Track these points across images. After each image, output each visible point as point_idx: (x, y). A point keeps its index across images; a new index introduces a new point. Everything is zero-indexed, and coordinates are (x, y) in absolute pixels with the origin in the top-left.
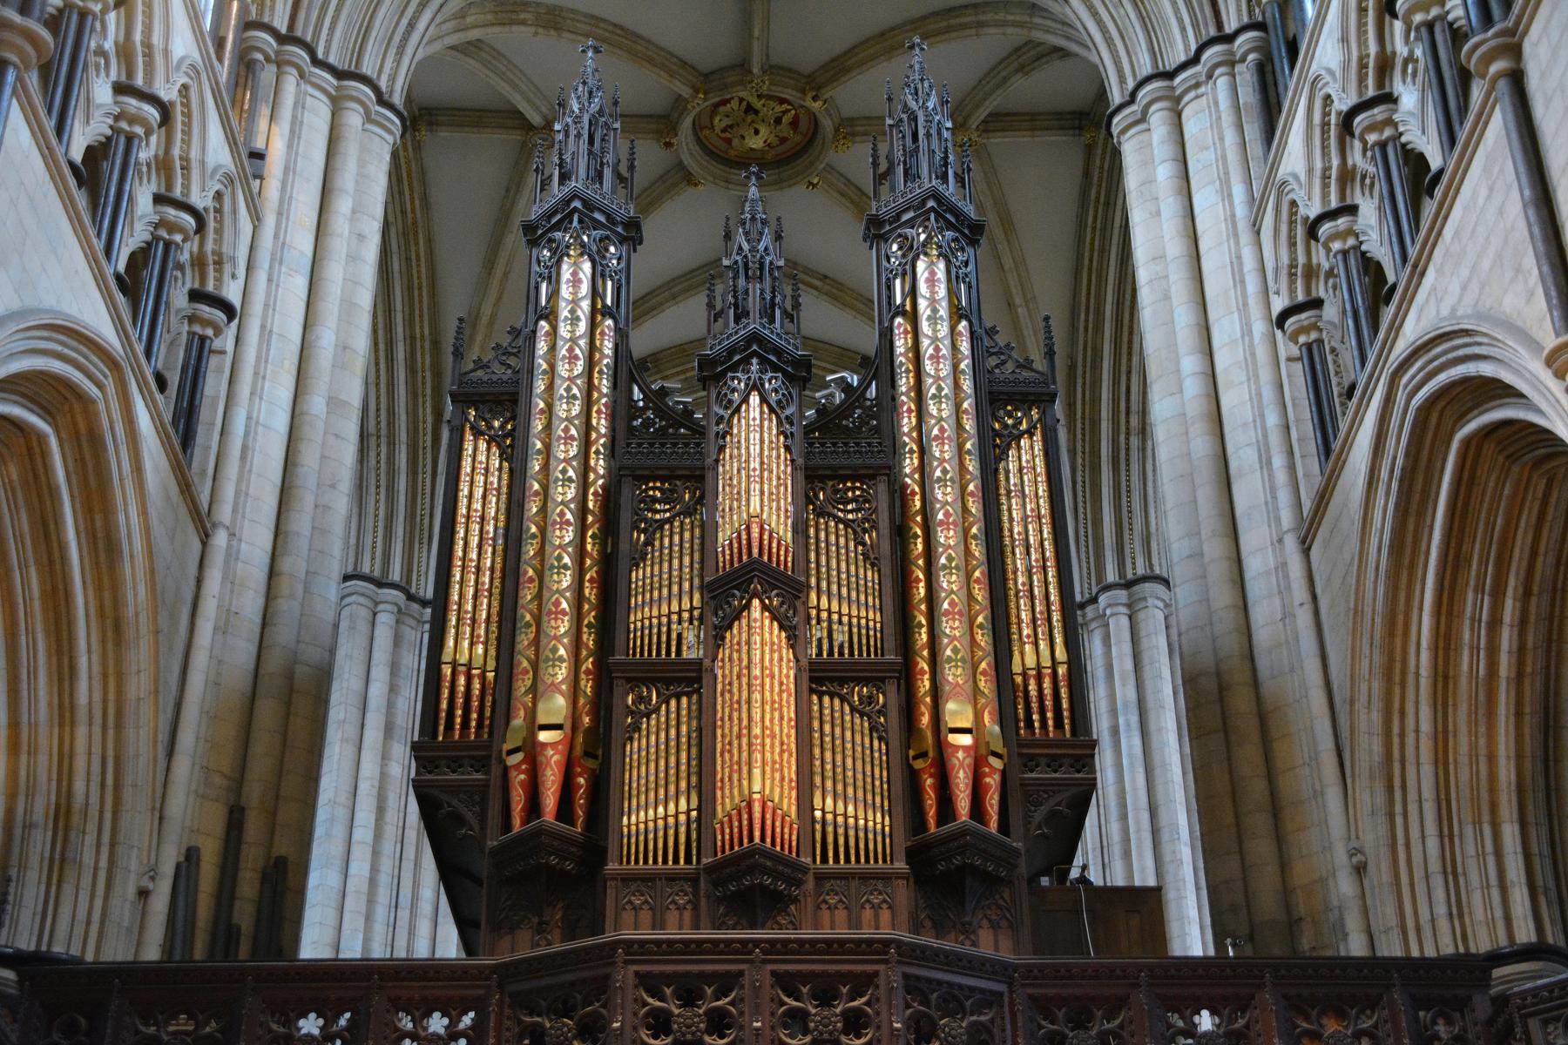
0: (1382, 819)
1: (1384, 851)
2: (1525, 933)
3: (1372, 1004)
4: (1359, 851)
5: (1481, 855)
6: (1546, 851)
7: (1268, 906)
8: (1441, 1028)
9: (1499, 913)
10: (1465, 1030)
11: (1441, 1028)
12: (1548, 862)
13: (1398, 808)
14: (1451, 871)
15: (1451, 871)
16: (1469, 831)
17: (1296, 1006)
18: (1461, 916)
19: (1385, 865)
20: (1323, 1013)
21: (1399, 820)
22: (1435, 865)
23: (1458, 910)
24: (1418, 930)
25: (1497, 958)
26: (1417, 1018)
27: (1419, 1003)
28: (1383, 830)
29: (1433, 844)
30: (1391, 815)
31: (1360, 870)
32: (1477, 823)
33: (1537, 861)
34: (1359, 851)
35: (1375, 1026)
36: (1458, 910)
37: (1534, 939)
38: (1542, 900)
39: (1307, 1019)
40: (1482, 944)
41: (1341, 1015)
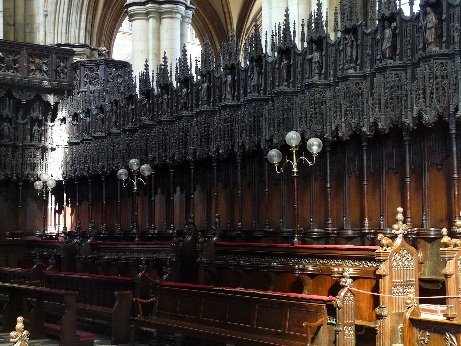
0: (54, 6)
1: (53, 14)
2: (82, 42)
3: (47, 57)
4: (46, 11)
5: (76, 20)
6: (91, 21)
7: (20, 19)
8: (62, 64)
9: (77, 35)
10: (66, 65)
11: (62, 64)
12: (91, 24)
13: (59, 3)
14: (68, 22)
15: (68, 22)
16: (74, 14)
17: (30, 55)
18: (68, 33)
19: (53, 17)
20: (36, 57)
21: (58, 6)
22: (65, 20)
23: (68, 32)
24: (58, 34)
25: (74, 46)
26: (57, 61)
27: (58, 58)
28: (54, 8)
29: (65, 15)
30: (57, 5)
31: (46, 15)
32: (77, 12)
33: (88, 24)
34: (46, 11)
35: (47, 62)
36: (68, 32)
37: (84, 43)
38: (87, 33)
39: (32, 58)
40: (72, 42)
41: (40, 58)
